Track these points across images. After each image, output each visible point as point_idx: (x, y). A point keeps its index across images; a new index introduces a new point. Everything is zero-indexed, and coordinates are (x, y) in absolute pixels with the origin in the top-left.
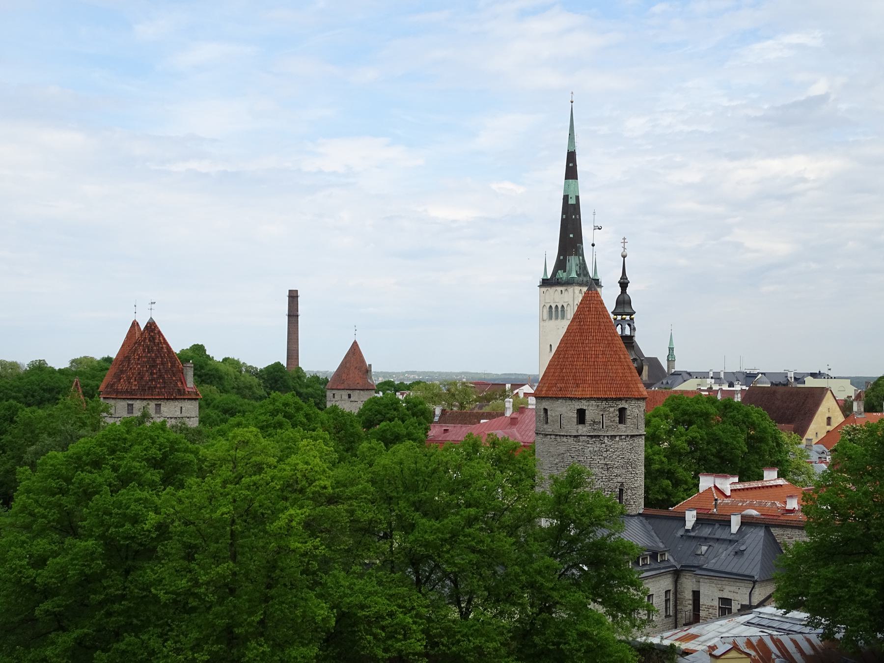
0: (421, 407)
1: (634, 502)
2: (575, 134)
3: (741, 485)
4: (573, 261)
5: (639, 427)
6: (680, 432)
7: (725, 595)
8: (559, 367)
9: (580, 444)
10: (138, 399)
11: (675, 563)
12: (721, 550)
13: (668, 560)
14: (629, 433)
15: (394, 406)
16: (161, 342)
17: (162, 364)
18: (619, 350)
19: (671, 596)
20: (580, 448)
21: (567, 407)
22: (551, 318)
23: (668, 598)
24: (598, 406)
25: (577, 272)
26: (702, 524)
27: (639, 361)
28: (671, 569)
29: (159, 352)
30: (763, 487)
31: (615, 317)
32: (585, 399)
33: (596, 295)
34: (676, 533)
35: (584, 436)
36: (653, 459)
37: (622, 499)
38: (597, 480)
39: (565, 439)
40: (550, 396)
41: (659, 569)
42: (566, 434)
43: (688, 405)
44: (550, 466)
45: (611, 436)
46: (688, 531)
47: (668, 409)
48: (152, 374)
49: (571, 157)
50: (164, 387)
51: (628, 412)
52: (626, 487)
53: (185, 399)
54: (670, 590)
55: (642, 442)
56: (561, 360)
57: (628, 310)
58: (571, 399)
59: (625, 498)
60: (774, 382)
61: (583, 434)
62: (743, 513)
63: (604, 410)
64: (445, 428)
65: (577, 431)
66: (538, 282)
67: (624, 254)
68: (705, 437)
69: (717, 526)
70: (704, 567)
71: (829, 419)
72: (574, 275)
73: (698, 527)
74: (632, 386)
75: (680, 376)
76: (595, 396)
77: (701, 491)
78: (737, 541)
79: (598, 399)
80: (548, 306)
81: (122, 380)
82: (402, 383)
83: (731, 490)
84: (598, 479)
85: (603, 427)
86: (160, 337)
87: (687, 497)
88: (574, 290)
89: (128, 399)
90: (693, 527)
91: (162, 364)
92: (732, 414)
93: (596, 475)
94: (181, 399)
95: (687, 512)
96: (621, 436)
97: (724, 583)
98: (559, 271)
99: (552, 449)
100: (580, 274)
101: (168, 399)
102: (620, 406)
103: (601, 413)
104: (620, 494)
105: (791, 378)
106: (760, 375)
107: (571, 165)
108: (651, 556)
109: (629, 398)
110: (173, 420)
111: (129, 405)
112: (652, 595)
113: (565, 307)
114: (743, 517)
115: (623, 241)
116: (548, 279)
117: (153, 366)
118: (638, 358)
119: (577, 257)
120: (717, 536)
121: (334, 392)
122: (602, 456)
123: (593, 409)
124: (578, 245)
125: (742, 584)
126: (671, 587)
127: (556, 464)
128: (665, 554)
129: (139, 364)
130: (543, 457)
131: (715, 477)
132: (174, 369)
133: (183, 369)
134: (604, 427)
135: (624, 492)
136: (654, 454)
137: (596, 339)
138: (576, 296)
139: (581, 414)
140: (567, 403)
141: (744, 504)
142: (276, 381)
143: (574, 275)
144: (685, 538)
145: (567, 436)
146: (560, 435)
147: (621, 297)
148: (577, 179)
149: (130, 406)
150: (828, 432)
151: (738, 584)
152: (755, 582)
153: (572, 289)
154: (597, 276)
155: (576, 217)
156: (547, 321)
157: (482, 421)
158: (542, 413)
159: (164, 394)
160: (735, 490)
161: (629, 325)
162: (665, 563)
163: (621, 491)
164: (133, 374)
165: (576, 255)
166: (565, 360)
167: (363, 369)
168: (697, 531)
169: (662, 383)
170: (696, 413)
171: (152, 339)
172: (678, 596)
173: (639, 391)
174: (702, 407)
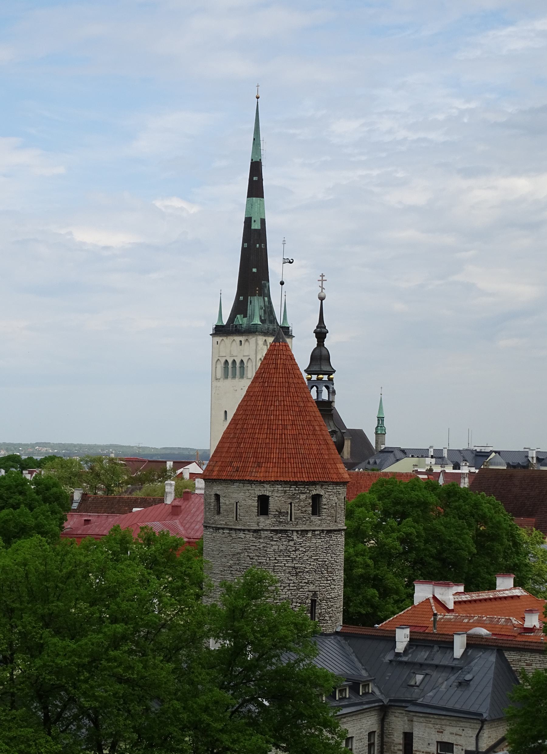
0: (55, 489)
1: (330, 617)
2: (261, 139)
3: (467, 596)
5: (338, 520)
6: (391, 526)
7: (446, 738)
8: (235, 440)
9: (261, 540)
11: (381, 697)
12: (440, 680)
13: (373, 693)
14: (325, 527)
15: (20, 488)
18: (313, 419)
19: (376, 740)
20: (262, 546)
21: (245, 493)
22: (226, 376)
23: (372, 741)
24: (285, 492)
25: (261, 317)
26: (417, 646)
27: (339, 433)
28: (377, 704)
30: (495, 599)
31: (310, 376)
32: (269, 482)
33: (284, 348)
34: (384, 657)
35: (267, 530)
36: (355, 562)
37: (315, 613)
38: (282, 588)
39: (242, 535)
40: (223, 478)
41: (361, 704)
42: (243, 528)
43: (402, 492)
44: (221, 568)
45: (302, 531)
46: (398, 655)
47: (375, 496)
51: (324, 500)
54: (374, 732)
56: (238, 432)
58: (251, 482)
59: (318, 611)
60: (511, 463)
61: (264, 528)
62: (470, 632)
63: (293, 497)
64: (86, 518)
65: (258, 525)
67: (322, 295)
68: (423, 534)
69: (436, 648)
70: (419, 701)
72: (257, 321)
73: (411, 650)
74: (329, 466)
75: (392, 454)
76: (282, 479)
77: (416, 603)
78: (461, 668)
79: (286, 483)
80: (223, 360)
82: (30, 459)
83: (455, 603)
84: (284, 587)
85: (291, 520)
87: (397, 611)
88: (256, 340)
90: (406, 650)
92: (457, 504)
93: (282, 582)
95: (397, 630)
96: (314, 531)
97: (443, 722)
98: (238, 316)
99: (224, 548)
100: (265, 320)
102: (314, 492)
103: (289, 501)
104: (312, 603)
105: (533, 458)
106: (494, 454)
107: (255, 178)
108: (351, 688)
109: (326, 482)
112: (352, 738)
113: (245, 362)
114: (469, 637)
116: (223, 326)
118: (337, 430)
119: (262, 298)
120: (436, 662)
122: (289, 556)
123: (279, 495)
124: (263, 282)
125: (467, 725)
126: (375, 728)
127: (230, 567)
128: (369, 684)
130: (213, 557)
131: (436, 585)
134: (293, 520)
135: (317, 604)
136: (356, 555)
137: (284, 405)
138: (259, 348)
140: (245, 488)
141: (471, 621)
143: (257, 321)
144: (394, 663)
145: (244, 530)
146: (235, 530)
147: (317, 351)
151: (462, 724)
152: (483, 722)
153: (254, 339)
154: (286, 322)
155: (260, 246)
156: (222, 379)
157: (135, 510)
158: (212, 501)
160: (460, 602)
161: (327, 387)
162: (369, 696)
163: (314, 602)
165: (260, 295)
166: (243, 431)
168: (410, 655)
169: (369, 463)
170: (412, 503)
172: (386, 739)
173: (338, 473)
174: (419, 494)
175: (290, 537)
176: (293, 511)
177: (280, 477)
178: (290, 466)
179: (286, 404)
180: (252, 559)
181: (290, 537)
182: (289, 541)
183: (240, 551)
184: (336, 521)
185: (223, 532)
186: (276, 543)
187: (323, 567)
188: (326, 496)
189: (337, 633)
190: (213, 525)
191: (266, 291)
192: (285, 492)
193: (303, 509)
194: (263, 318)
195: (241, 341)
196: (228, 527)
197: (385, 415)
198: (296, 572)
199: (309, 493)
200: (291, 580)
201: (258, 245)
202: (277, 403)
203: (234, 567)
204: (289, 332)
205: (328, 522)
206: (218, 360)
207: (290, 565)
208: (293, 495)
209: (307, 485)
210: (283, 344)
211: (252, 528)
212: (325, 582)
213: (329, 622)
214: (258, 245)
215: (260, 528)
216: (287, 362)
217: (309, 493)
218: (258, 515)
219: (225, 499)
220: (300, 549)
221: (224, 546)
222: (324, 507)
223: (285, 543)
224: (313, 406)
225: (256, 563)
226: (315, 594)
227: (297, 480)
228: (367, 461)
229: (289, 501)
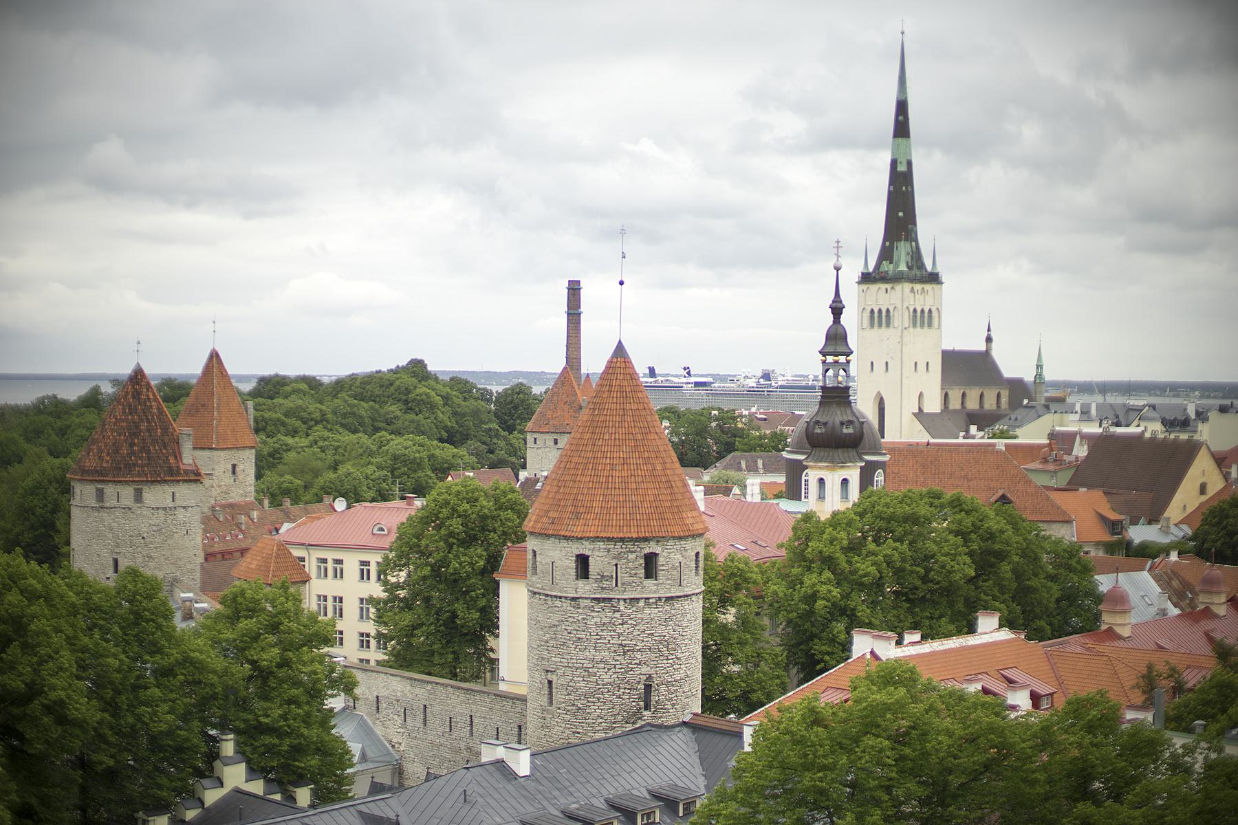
4: (902, 251)
8: (555, 483)
9: (580, 611)
10: (109, 481)
14: (662, 594)
16: (149, 399)
17: (148, 431)
21: (561, 551)
24: (609, 550)
27: (857, 424)
29: (144, 413)
32: (588, 538)
35: (586, 598)
38: (606, 670)
39: (558, 603)
42: (559, 594)
45: (631, 599)
48: (135, 444)
49: (902, 107)
50: (148, 465)
52: (656, 680)
53: (179, 481)
55: (696, 607)
57: (841, 349)
58: (567, 538)
59: (654, 698)
61: (584, 596)
63: (619, 556)
66: (856, 276)
72: (903, 267)
76: (603, 534)
79: (609, 539)
80: (869, 310)
81: (91, 454)
84: (609, 669)
85: (616, 585)
86: (148, 390)
89: (96, 481)
91: (148, 431)
93: (605, 662)
94: (173, 481)
95: (745, 727)
96: (648, 599)
100: (913, 266)
101: (152, 482)
102: (647, 551)
103: (615, 562)
107: (901, 118)
110: (161, 511)
111: (98, 489)
113: (891, 310)
115: (836, 245)
116: (869, 274)
117: (134, 433)
118: (855, 420)
119: (908, 244)
121: (536, 435)
122: (614, 631)
124: (910, 226)
129: (116, 431)
132: (166, 437)
133: (178, 439)
134: (619, 585)
135: (654, 689)
137: (615, 439)
139: (583, 562)
140: (561, 546)
142: (516, 408)
143: (903, 267)
145: (561, 597)
146: (551, 596)
148: (909, 137)
149: (100, 495)
150: (1201, 505)
156: (868, 329)
159: (146, 475)
163: (648, 688)
164: (106, 446)
165: (906, 240)
167: (576, 404)
169: (1010, 419)
171: (137, 395)
175: (615, 607)
176: (619, 574)
177: (601, 531)
178: (615, 518)
179: (617, 437)
180: (570, 633)
181: (615, 607)
182: (614, 612)
183: (557, 623)
184: (680, 585)
185: (540, 599)
186: (597, 614)
187: (661, 644)
188: (664, 554)
189: (685, 722)
190: (531, 589)
191: (913, 236)
192: (609, 550)
193: (633, 572)
194: (910, 264)
195: (887, 290)
196: (543, 592)
197: (1045, 362)
198: (624, 650)
199: (640, 552)
200: (618, 661)
201: (904, 188)
202: (607, 437)
203: (551, 642)
204: (938, 278)
205: (668, 587)
206: (864, 309)
207: (615, 642)
208: (619, 554)
209: (636, 542)
210: (623, 360)
211: (569, 595)
212: (665, 662)
213: (671, 711)
214: (904, 188)
215: (578, 596)
216: (625, 383)
217: (640, 552)
218: (577, 579)
219: (541, 557)
220: (629, 622)
221: (540, 615)
222: (662, 568)
223: (609, 614)
224: (656, 438)
225: (574, 639)
227: (621, 535)
228: (1008, 417)
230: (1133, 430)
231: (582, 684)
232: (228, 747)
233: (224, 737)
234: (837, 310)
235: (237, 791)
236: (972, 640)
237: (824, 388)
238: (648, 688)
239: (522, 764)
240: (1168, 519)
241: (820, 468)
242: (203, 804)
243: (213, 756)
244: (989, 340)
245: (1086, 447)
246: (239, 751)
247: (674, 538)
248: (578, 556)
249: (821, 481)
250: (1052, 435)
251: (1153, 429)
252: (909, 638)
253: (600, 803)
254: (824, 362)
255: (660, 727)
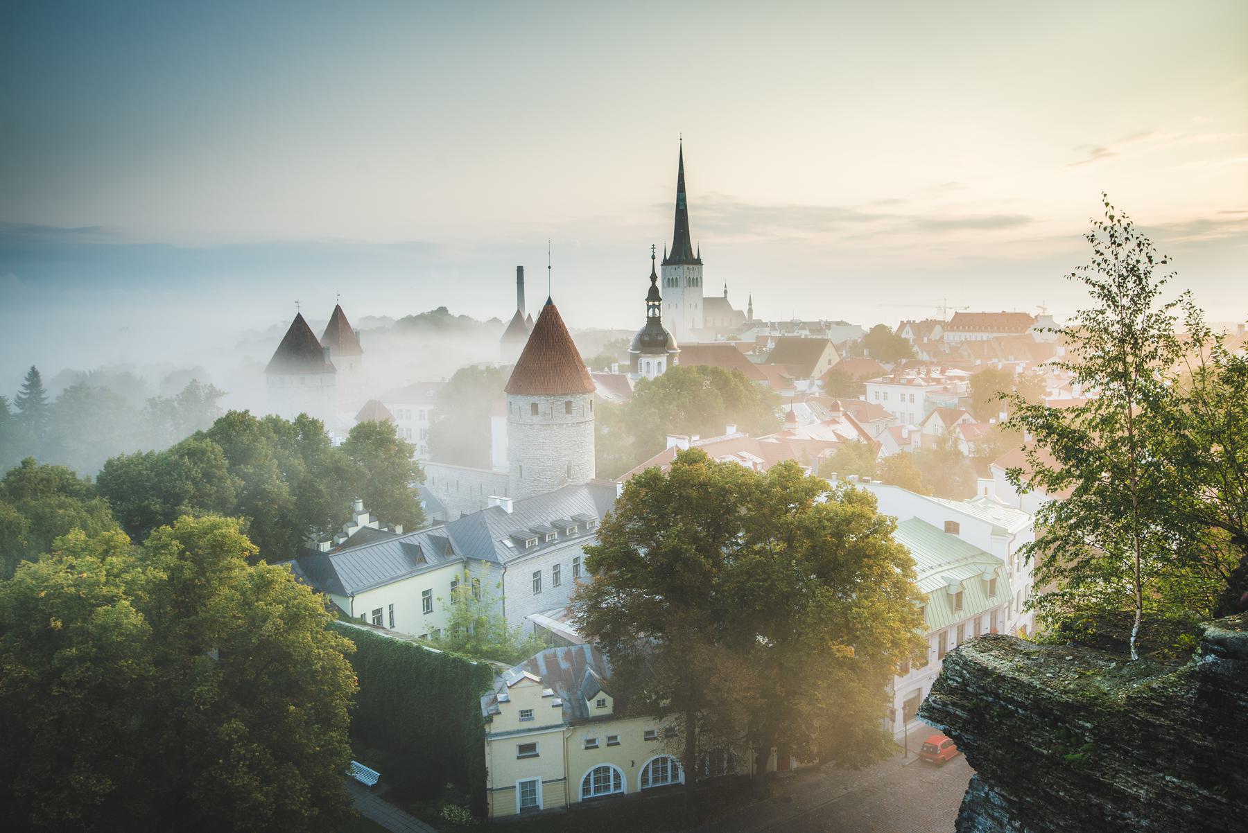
22: (669, 286)
24: (548, 400)
30: (720, 442)
55: (592, 426)
59: (572, 472)
63: (553, 403)
71: (830, 361)
103: (550, 406)
150: (829, 369)
161: (659, 309)
163: (569, 468)
192: (548, 400)
218: (532, 415)
226: (570, 462)
229: (550, 406)
230: (795, 334)
231: (537, 467)
232: (360, 506)
233: (357, 501)
234: (654, 278)
235: (365, 527)
236: (724, 438)
237: (648, 317)
238: (569, 468)
239: (509, 508)
240: (813, 377)
241: (647, 357)
242: (348, 535)
243: (352, 511)
244: (726, 292)
245: (774, 344)
246: (365, 506)
247: (580, 393)
248: (532, 404)
249: (648, 363)
250: (757, 338)
251: (804, 334)
252: (693, 438)
253: (548, 525)
254: (648, 305)
255: (575, 486)
